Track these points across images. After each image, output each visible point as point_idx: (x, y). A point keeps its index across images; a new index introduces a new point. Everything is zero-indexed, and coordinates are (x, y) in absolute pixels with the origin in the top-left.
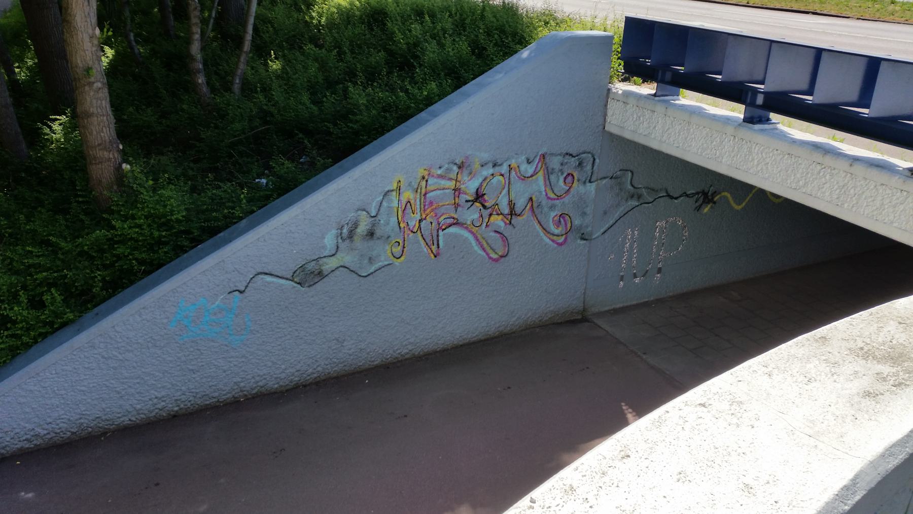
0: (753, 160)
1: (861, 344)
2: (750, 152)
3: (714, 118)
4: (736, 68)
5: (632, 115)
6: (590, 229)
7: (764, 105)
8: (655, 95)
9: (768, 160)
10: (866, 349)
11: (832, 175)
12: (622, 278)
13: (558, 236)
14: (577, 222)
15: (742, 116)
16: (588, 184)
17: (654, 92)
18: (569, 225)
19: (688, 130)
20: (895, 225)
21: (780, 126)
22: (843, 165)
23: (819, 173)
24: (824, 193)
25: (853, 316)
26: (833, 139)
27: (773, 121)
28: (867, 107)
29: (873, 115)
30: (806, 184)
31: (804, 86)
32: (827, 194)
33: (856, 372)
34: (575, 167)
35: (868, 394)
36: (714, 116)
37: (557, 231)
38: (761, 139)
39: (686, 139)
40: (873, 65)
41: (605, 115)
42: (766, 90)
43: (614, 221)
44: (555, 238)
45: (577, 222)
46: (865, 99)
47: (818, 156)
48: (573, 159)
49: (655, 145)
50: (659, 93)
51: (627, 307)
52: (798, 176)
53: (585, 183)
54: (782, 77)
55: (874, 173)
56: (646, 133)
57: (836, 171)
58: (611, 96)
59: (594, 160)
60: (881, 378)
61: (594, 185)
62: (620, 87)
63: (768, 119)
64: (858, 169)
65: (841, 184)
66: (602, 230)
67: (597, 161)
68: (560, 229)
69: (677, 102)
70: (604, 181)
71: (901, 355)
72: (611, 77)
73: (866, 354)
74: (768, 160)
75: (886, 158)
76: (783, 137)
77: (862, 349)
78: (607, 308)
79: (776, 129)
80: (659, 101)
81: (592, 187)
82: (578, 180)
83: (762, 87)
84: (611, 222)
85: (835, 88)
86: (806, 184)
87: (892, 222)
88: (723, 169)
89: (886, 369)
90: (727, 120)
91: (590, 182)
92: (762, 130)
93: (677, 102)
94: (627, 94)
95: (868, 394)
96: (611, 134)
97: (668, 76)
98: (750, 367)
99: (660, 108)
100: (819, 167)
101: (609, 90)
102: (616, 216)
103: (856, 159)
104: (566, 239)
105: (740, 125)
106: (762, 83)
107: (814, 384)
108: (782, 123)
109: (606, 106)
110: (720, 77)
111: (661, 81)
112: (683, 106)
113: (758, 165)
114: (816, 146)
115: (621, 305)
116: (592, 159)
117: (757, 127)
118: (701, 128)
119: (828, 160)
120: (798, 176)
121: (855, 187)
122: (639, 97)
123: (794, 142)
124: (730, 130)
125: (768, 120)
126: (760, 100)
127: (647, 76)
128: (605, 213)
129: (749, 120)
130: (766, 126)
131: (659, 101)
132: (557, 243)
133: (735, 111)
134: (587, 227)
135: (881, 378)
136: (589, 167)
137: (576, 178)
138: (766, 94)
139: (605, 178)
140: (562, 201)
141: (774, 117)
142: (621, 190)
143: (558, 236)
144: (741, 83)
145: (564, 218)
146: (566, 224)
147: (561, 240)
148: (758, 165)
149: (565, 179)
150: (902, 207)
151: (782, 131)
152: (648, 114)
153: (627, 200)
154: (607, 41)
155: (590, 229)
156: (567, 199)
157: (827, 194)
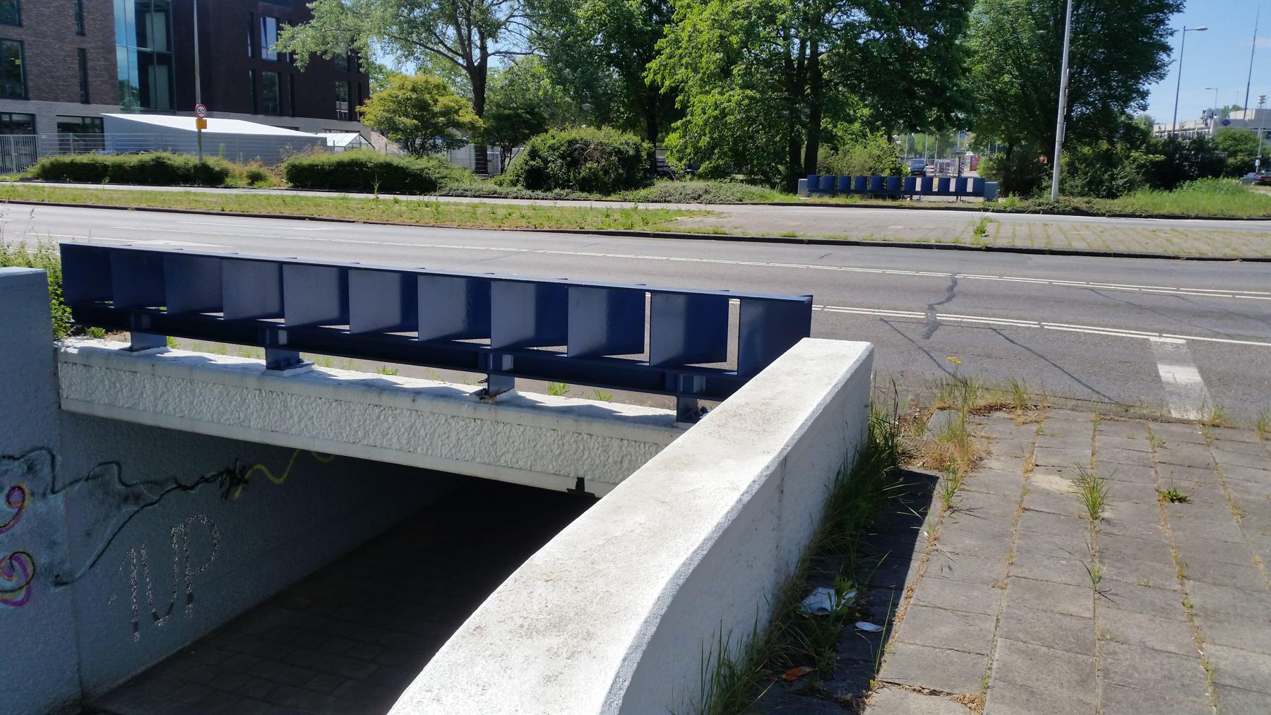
0: (291, 416)
1: (519, 622)
2: (286, 406)
3: (225, 369)
4: (245, 300)
5: (102, 381)
6: (67, 566)
7: (289, 345)
8: (131, 349)
9: (311, 413)
10: (526, 625)
11: (394, 417)
12: (136, 627)
13: (12, 591)
14: (43, 560)
15: (263, 362)
16: (51, 497)
17: (128, 345)
18: (30, 569)
19: (193, 391)
20: (478, 460)
21: (316, 367)
22: (403, 403)
23: (379, 417)
24: (390, 440)
25: (499, 589)
26: (384, 372)
27: (306, 362)
28: (487, 335)
29: (423, 338)
30: (366, 435)
31: (334, 312)
32: (394, 441)
33: (527, 658)
34: (23, 475)
35: (548, 679)
36: (225, 366)
37: (9, 585)
38: (295, 387)
39: (192, 403)
40: (409, 281)
41: (57, 389)
42: (289, 324)
43: (105, 542)
44: (8, 596)
45: (43, 560)
46: (410, 320)
47: (372, 398)
48: (16, 463)
49: (147, 420)
50: (138, 346)
51: (155, 667)
52: (355, 425)
53: (44, 495)
54: (305, 307)
55: (441, 406)
56: (129, 405)
57: (399, 411)
58: (61, 358)
59: (53, 457)
60: (553, 654)
61: (60, 496)
62: (73, 344)
63: (299, 361)
64: (422, 403)
65: (408, 425)
66: (89, 563)
67: (59, 458)
68: (15, 579)
69: (166, 355)
70: (77, 487)
71: (562, 618)
72: (55, 331)
73: (528, 631)
74: (311, 413)
75: (448, 385)
76: (325, 380)
77: (522, 626)
78: (121, 681)
79: (313, 371)
80: (139, 357)
81: (58, 501)
82: (33, 494)
83: (282, 321)
84: (100, 547)
85: (373, 311)
86: (366, 435)
87: (474, 459)
88: (253, 435)
89: (553, 641)
90: (244, 370)
91: (53, 492)
92: (294, 376)
93: (166, 355)
94: (86, 352)
95: (548, 679)
96: (72, 415)
97: (146, 321)
98: (412, 698)
99: (143, 367)
100: (377, 410)
101: (56, 350)
102: (108, 533)
103: (417, 393)
104: (28, 593)
105: (263, 374)
106: (281, 315)
107: (490, 691)
108: (531, 391)
109: (56, 374)
110: (221, 314)
111: (135, 329)
112: (176, 358)
113: (300, 422)
114: (368, 385)
115: (143, 668)
116: (49, 457)
117: (287, 373)
118: (210, 384)
119: (386, 400)
120: (355, 425)
121: (424, 425)
122: (109, 354)
123: (340, 384)
124: (251, 382)
125: (299, 362)
126: (283, 338)
127: (112, 324)
128: (88, 534)
129: (275, 365)
130: (298, 370)
131: (139, 357)
132: (15, 604)
133: (255, 357)
134: (62, 563)
135: (553, 654)
136: (47, 471)
137: (27, 491)
138: (290, 330)
139: (76, 481)
140: (9, 533)
141: (306, 357)
142: (106, 493)
143: (12, 591)
144: (252, 320)
145: (18, 559)
146: (24, 569)
147: (20, 596)
148: (300, 422)
149: (8, 496)
150: (479, 439)
151: (320, 374)
152: (126, 378)
153: (118, 508)
154: (37, 280)
155: (67, 566)
156: (18, 529)
157: (394, 441)
